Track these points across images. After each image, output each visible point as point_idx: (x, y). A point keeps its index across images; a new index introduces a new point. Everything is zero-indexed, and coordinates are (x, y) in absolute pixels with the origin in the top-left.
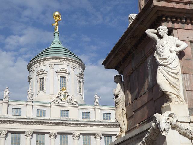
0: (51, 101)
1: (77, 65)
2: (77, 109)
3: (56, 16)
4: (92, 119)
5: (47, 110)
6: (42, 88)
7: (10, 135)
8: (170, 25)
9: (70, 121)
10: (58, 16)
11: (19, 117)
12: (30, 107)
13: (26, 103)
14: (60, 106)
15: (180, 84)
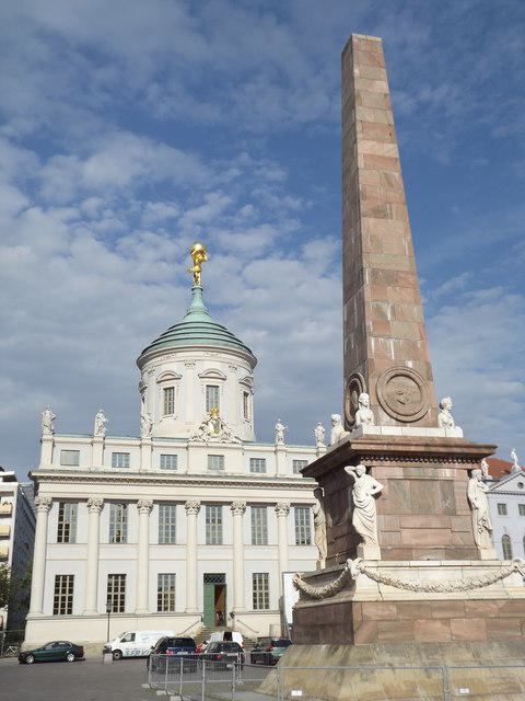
0: (188, 435)
1: (240, 360)
2: (240, 452)
3: (197, 253)
4: (270, 472)
5: (181, 454)
6: (169, 409)
7: (107, 506)
8: (369, 463)
9: (227, 477)
10: (202, 252)
11: (125, 470)
12: (147, 450)
13: (138, 442)
14: (208, 447)
15: (375, 527)
